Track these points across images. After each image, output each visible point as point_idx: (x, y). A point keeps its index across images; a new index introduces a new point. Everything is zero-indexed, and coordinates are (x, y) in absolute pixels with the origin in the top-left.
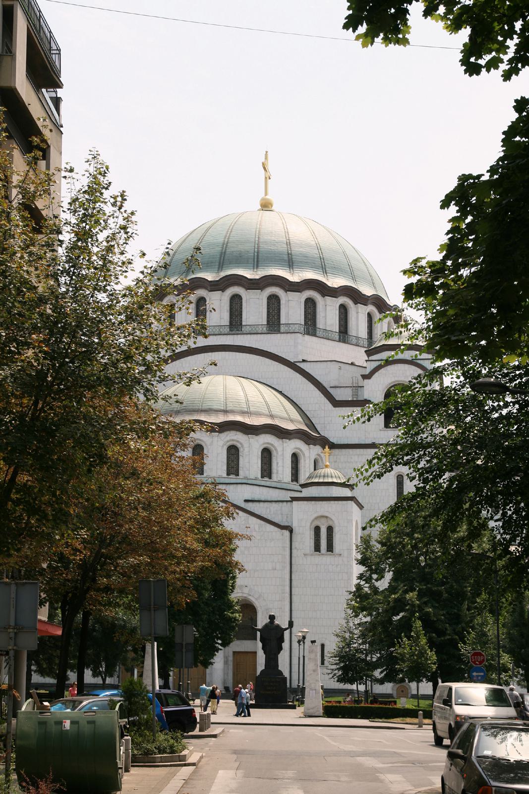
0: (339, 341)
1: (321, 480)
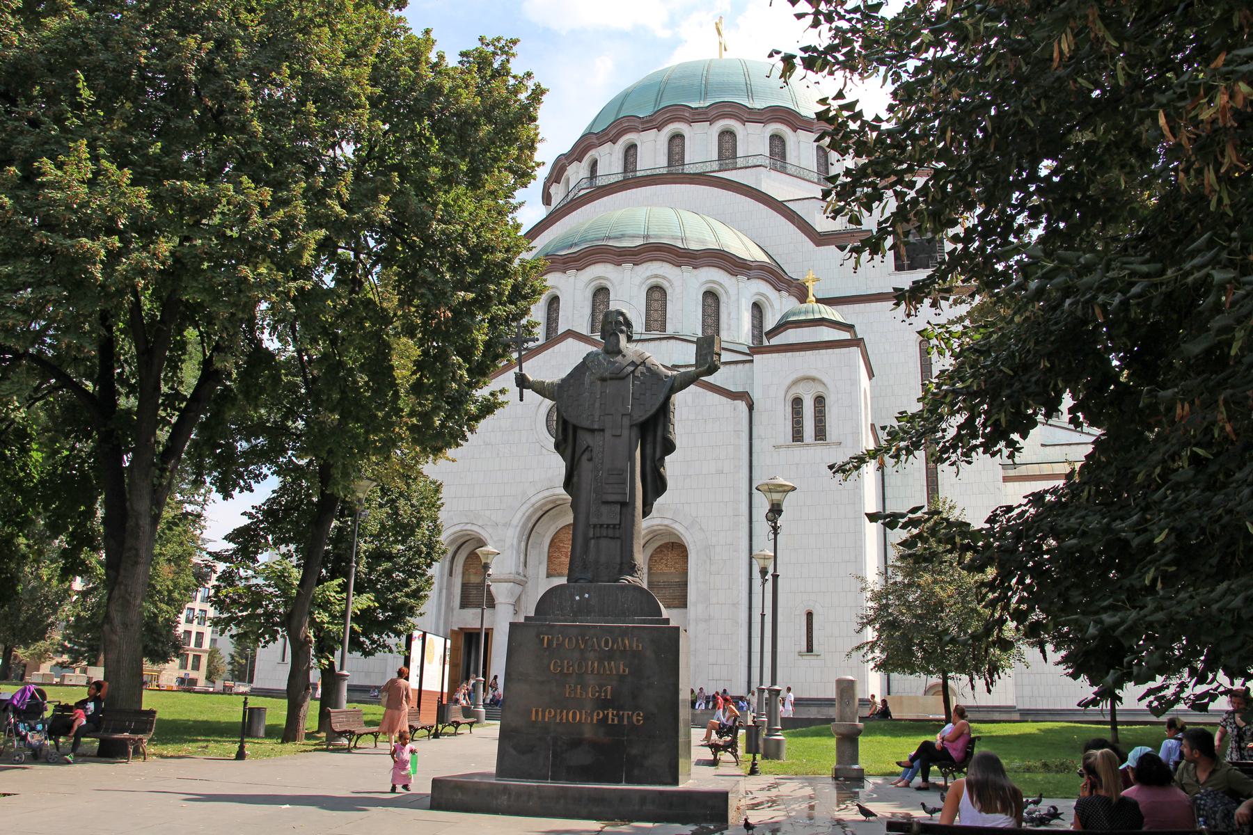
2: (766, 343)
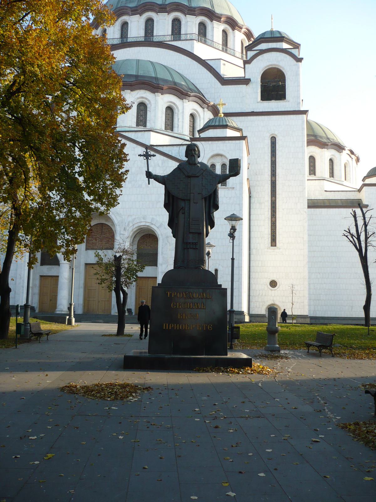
0: (223, 51)
2: (197, 135)
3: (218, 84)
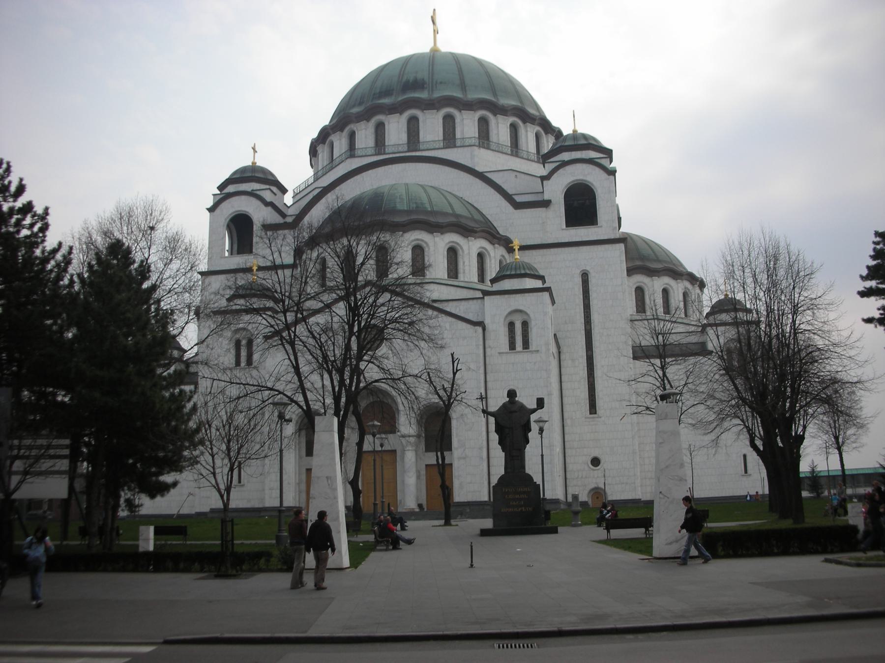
0: (512, 155)
1: (513, 273)
3: (510, 208)
